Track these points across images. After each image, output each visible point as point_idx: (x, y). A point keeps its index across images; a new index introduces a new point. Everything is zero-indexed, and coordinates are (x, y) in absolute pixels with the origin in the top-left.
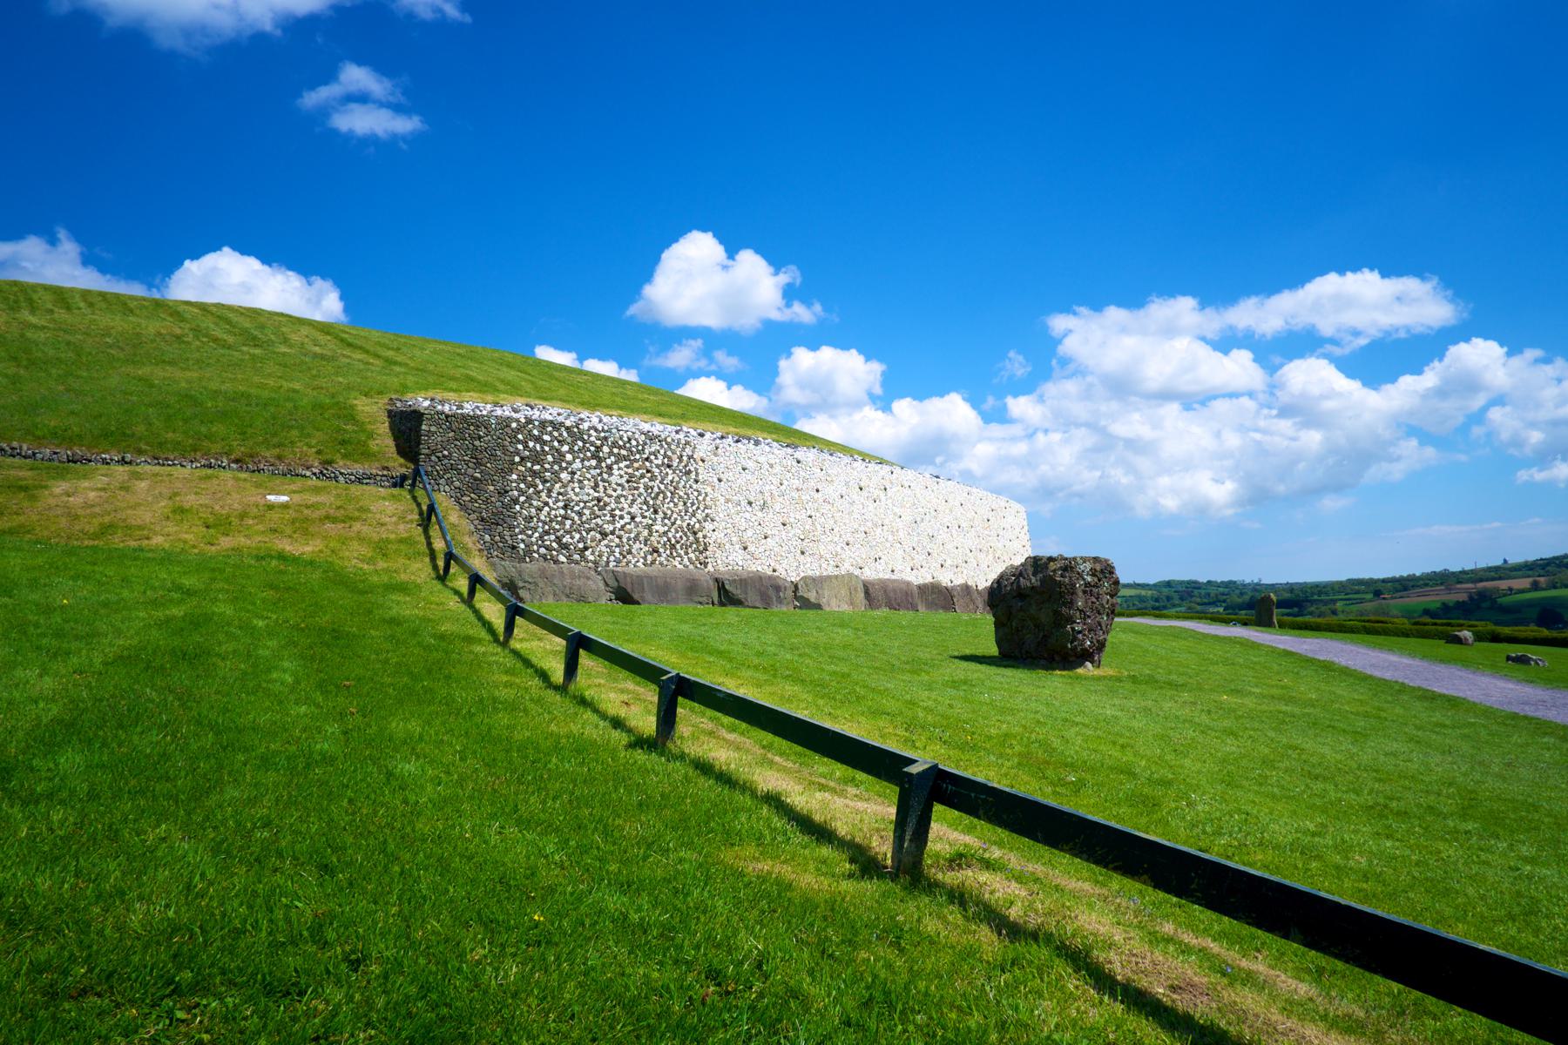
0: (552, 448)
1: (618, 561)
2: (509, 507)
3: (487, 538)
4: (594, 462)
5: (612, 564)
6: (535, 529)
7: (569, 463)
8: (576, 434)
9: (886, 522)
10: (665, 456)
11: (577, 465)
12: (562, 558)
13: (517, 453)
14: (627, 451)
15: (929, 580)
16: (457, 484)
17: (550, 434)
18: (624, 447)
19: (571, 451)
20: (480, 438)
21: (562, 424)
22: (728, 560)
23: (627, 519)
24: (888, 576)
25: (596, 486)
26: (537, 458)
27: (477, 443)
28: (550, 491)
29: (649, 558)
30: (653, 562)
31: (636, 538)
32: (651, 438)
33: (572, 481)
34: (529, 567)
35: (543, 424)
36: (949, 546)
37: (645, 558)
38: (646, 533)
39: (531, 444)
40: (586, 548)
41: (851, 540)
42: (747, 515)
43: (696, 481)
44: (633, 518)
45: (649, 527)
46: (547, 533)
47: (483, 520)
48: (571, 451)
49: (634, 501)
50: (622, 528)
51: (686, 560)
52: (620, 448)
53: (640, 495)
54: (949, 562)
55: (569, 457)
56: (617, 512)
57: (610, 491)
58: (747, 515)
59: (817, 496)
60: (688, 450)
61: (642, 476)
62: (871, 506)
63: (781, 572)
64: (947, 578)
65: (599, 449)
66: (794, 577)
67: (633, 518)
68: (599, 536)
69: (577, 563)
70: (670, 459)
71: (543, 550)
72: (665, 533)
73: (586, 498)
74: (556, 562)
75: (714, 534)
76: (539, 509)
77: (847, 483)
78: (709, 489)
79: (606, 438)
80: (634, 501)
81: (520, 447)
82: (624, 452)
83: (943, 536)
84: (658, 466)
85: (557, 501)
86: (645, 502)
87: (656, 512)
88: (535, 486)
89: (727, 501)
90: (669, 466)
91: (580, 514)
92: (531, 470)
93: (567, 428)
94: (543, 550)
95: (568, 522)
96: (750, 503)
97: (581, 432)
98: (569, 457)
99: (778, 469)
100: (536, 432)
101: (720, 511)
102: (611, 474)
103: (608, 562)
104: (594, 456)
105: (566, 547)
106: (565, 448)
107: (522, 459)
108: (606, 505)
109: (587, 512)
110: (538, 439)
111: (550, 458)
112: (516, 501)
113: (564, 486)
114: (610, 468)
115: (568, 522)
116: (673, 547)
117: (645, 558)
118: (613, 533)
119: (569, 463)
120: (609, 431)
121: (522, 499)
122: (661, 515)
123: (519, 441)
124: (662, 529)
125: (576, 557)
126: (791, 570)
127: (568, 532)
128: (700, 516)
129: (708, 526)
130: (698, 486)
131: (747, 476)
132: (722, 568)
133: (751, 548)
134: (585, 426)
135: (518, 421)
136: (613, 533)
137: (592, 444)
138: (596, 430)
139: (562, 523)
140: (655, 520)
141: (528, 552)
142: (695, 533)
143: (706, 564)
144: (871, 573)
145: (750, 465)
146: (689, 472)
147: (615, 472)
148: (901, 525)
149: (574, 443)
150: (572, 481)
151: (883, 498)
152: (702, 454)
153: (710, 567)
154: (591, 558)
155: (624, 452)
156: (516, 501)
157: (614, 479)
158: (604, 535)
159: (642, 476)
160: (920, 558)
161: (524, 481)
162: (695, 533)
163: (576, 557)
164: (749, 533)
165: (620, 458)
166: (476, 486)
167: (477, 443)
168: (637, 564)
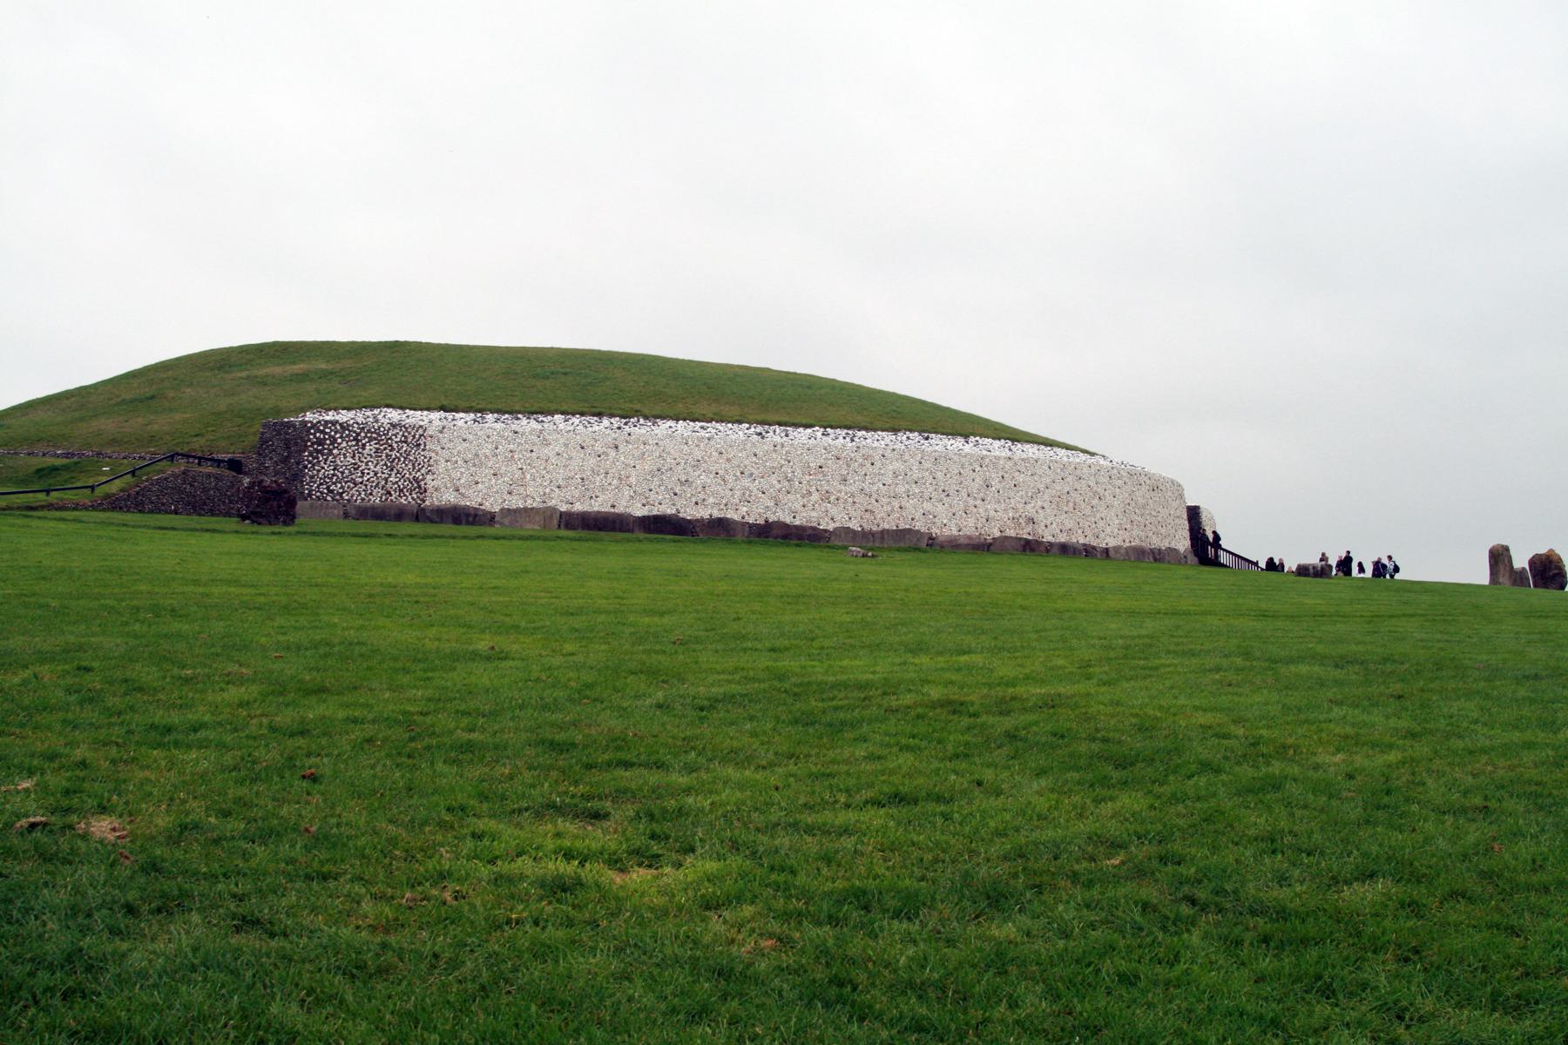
14: (377, 435)
15: (670, 511)
22: (442, 495)
24: (607, 509)
26: (321, 442)
62: (593, 461)
63: (487, 506)
64: (690, 513)
66: (497, 509)
77: (566, 445)
101: (441, 467)
126: (493, 505)
129: (429, 477)
131: (465, 445)
133: (462, 490)
141: (310, 495)
144: (578, 507)
165: (371, 440)
166: (285, 460)
168: (376, 499)
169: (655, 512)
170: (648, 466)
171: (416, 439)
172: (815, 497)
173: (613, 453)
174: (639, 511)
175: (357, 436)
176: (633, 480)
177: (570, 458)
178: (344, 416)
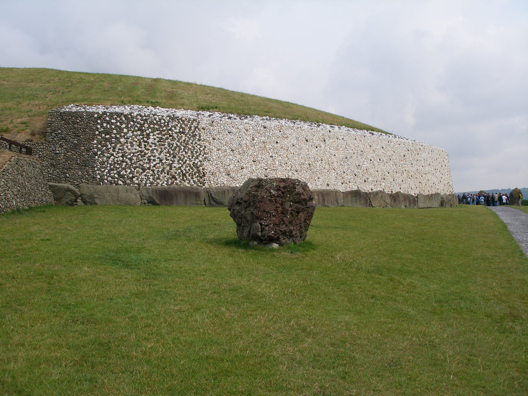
0: (116, 126)
1: (152, 183)
2: (92, 157)
3: (80, 173)
4: (139, 133)
5: (148, 185)
6: (106, 168)
7: (126, 134)
8: (129, 118)
9: (325, 158)
10: (181, 127)
11: (130, 134)
12: (120, 182)
13: (97, 129)
14: (159, 126)
15: (355, 188)
16: (65, 147)
17: (116, 119)
18: (157, 124)
19: (127, 127)
20: (78, 123)
21: (122, 114)
23: (158, 161)
24: (325, 187)
25: (140, 143)
27: (76, 126)
28: (114, 148)
29: (170, 181)
30: (172, 183)
31: (163, 171)
32: (173, 118)
33: (127, 142)
34: (101, 187)
35: (112, 114)
36: (372, 171)
37: (167, 181)
38: (168, 168)
39: (105, 125)
40: (133, 177)
41: (299, 168)
42: (231, 157)
43: (199, 140)
44: (161, 161)
45: (170, 165)
46: (112, 170)
47: (78, 164)
48: (127, 127)
49: (161, 152)
50: (154, 166)
51: (192, 181)
52: (154, 124)
53: (165, 148)
54: (371, 179)
55: (125, 130)
56: (152, 158)
57: (148, 147)
58: (231, 157)
59: (276, 145)
60: (195, 124)
61: (167, 138)
62: (314, 150)
64: (366, 188)
65: (142, 125)
67: (161, 161)
68: (141, 171)
69: (129, 184)
70: (183, 128)
71: (110, 179)
72: (180, 168)
73: (134, 151)
74: (117, 184)
75: (208, 167)
76: (109, 158)
77: (297, 139)
78: (207, 144)
79: (146, 120)
80: (161, 152)
81: (99, 126)
82: (156, 126)
83: (366, 164)
84: (176, 133)
85: (118, 153)
86: (168, 152)
87: (175, 157)
88: (107, 146)
89: (218, 150)
90: (183, 133)
91: (131, 159)
92: (103, 138)
93: (125, 116)
94: (110, 179)
95: (124, 164)
96: (233, 151)
97: (133, 117)
98: (125, 130)
99: (251, 132)
100: (108, 119)
102: (149, 138)
103: (146, 184)
104: (139, 130)
105: (123, 176)
106: (124, 126)
107: (100, 132)
108: (145, 154)
109: (134, 158)
110: (108, 123)
111: (115, 131)
112: (96, 154)
113: (122, 145)
114: (148, 135)
115: (124, 164)
116: (184, 175)
117: (167, 181)
118: (149, 168)
119: (126, 134)
120: (149, 116)
121: (99, 153)
122: (177, 158)
123: (98, 123)
124: (178, 166)
125: (128, 181)
127: (123, 169)
128: (200, 158)
130: (201, 143)
132: (214, 186)
133: (233, 175)
134: (135, 114)
135: (98, 113)
136: (149, 168)
137: (139, 123)
138: (141, 116)
139: (121, 165)
140: (174, 161)
141: (102, 179)
142: (197, 168)
143: (204, 185)
145: (234, 130)
146: (196, 135)
147: (152, 137)
148: (335, 160)
149: (128, 123)
150: (127, 142)
151: (323, 146)
152: (203, 126)
153: (206, 185)
154: (137, 182)
155: (156, 126)
156: (96, 154)
157: (150, 141)
158: (144, 170)
159: (167, 138)
160: (347, 178)
161: (100, 144)
162: (197, 168)
163: (128, 181)
164: (232, 167)
167: (76, 126)
168: (163, 183)
169: (349, 190)
170: (341, 155)
171: (191, 130)
172: (405, 176)
173: (323, 146)
174: (342, 189)
175: (142, 126)
176: (335, 165)
177: (301, 149)
178: (118, 109)
